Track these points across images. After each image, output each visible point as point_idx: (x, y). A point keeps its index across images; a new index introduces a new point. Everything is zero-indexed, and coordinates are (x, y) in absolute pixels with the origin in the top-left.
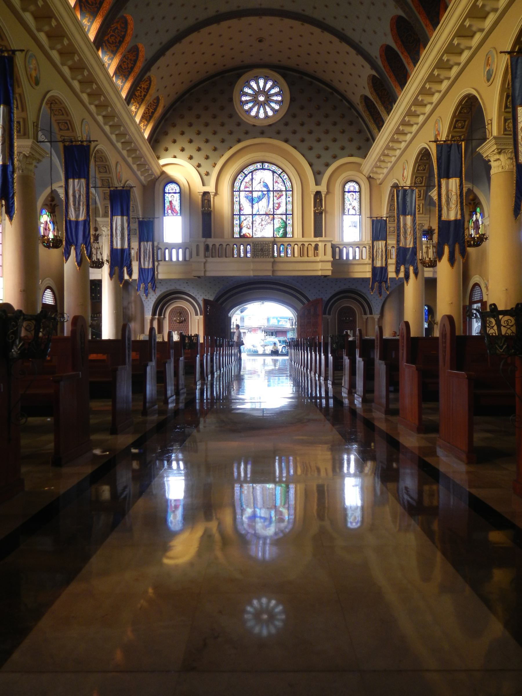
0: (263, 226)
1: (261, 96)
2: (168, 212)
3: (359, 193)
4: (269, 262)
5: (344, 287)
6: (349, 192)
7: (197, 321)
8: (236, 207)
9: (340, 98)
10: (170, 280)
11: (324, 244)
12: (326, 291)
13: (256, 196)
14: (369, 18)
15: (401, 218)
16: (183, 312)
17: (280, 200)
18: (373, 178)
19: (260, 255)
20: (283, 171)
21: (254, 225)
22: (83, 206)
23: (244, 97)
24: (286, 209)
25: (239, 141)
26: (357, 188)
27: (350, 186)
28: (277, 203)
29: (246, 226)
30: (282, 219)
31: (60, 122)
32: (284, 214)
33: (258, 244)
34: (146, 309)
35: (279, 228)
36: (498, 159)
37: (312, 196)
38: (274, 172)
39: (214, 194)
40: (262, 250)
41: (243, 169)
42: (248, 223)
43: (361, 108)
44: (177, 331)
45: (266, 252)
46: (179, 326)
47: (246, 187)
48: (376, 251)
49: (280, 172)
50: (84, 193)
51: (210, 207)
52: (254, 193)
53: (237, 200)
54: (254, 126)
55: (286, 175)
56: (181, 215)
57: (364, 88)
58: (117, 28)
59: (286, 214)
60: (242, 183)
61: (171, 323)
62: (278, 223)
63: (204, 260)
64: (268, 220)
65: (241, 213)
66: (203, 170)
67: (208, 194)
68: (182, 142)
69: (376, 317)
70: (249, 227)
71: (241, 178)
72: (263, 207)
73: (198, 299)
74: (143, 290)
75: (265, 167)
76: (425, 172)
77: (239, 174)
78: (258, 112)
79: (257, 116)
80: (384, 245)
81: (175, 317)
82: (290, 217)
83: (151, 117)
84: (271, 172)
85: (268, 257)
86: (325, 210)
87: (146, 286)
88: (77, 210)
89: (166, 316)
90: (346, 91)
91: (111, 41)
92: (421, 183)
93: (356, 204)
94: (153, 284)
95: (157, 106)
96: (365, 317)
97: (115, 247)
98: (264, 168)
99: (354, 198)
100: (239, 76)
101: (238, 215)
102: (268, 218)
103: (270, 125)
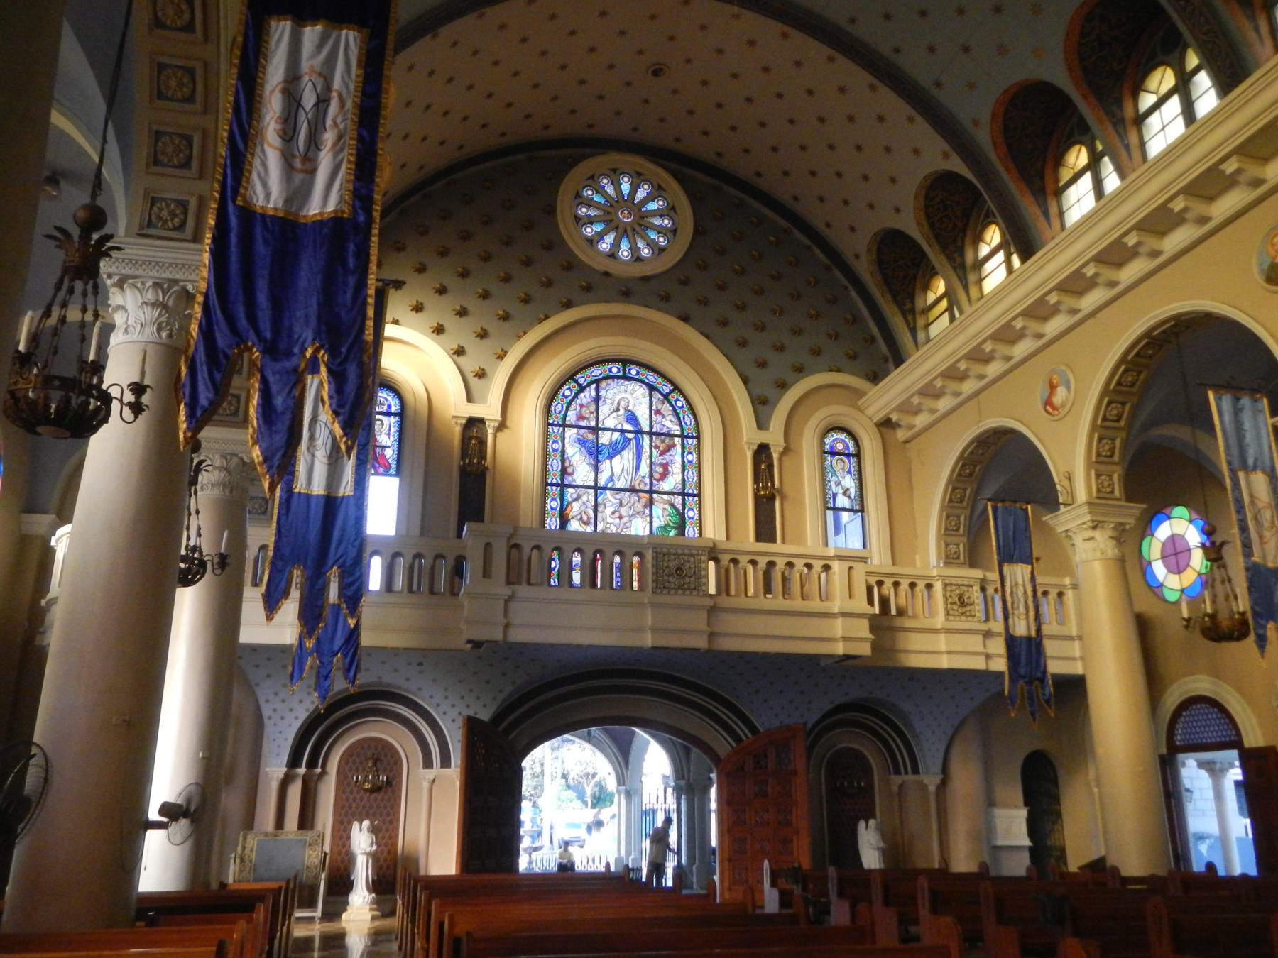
0: (625, 520)
1: (626, 212)
4: (699, 608)
5: (856, 693)
6: (833, 453)
7: (426, 785)
8: (555, 464)
10: (384, 648)
11: (846, 565)
12: (809, 702)
13: (607, 443)
15: (1241, 475)
17: (667, 457)
20: (676, 388)
21: (599, 515)
22: (338, 148)
23: (584, 210)
24: (683, 480)
25: (568, 305)
27: (834, 441)
28: (661, 464)
29: (579, 517)
30: (673, 505)
32: (678, 494)
33: (669, 554)
34: (268, 747)
37: (749, 454)
38: (651, 388)
39: (496, 424)
42: (583, 508)
43: (865, 268)
44: (367, 817)
45: (690, 577)
46: (369, 801)
47: (581, 417)
48: (1012, 593)
49: (666, 390)
50: (352, 86)
51: (483, 455)
52: (600, 432)
54: (607, 274)
56: (398, 473)
57: (897, 210)
59: (683, 494)
61: (344, 792)
62: (661, 515)
63: (507, 591)
64: (636, 505)
65: (566, 482)
66: (470, 363)
67: (480, 425)
69: (932, 781)
70: (585, 518)
71: (567, 393)
72: (625, 472)
74: (312, 681)
75: (630, 372)
76: (1134, 390)
78: (616, 245)
79: (612, 255)
80: (1029, 576)
81: (357, 770)
82: (689, 500)
84: (644, 386)
85: (698, 595)
86: (780, 491)
87: (326, 661)
88: (298, 163)
90: (828, 225)
92: (1118, 421)
93: (849, 482)
94: (348, 659)
96: (896, 780)
97: (300, 486)
101: (557, 485)
102: (636, 498)
103: (646, 279)
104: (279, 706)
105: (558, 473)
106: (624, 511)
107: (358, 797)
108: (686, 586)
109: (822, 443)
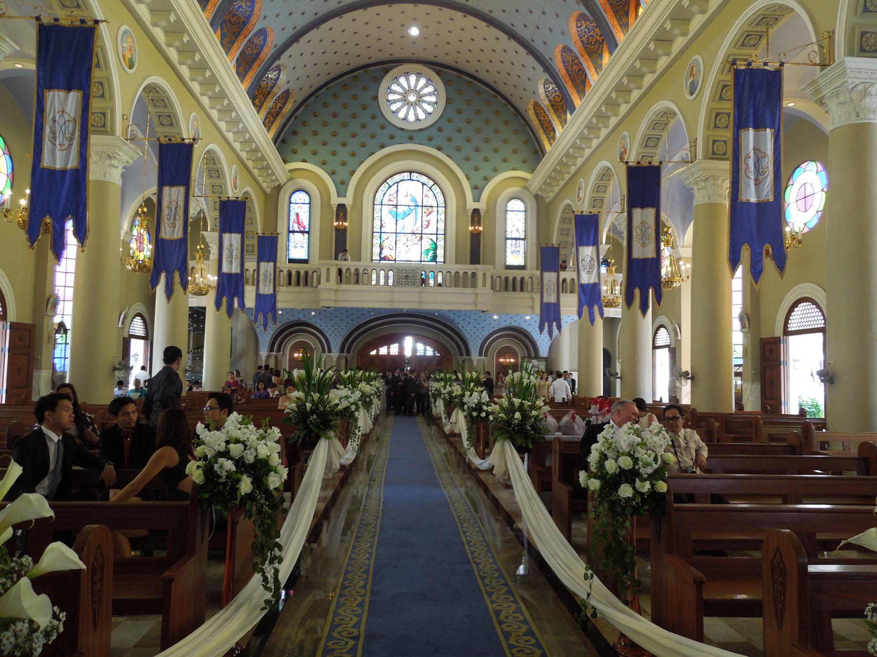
6: (512, 211)
8: (377, 224)
9: (505, 102)
14: (544, 13)
17: (429, 217)
18: (541, 197)
24: (437, 228)
30: (431, 240)
31: (161, 116)
33: (402, 270)
34: (261, 344)
35: (428, 250)
36: (705, 188)
38: (423, 184)
40: (407, 277)
41: (387, 180)
42: (390, 243)
52: (398, 207)
55: (437, 188)
58: (241, 6)
59: (437, 234)
60: (385, 195)
62: (427, 244)
68: (314, 143)
70: (391, 248)
71: (384, 189)
73: (325, 333)
77: (382, 184)
79: (405, 119)
83: (278, 113)
91: (233, 23)
95: (286, 101)
98: (412, 178)
100: (387, 71)
103: (421, 130)
105: (379, 227)
106: (409, 243)
109: (506, 206)
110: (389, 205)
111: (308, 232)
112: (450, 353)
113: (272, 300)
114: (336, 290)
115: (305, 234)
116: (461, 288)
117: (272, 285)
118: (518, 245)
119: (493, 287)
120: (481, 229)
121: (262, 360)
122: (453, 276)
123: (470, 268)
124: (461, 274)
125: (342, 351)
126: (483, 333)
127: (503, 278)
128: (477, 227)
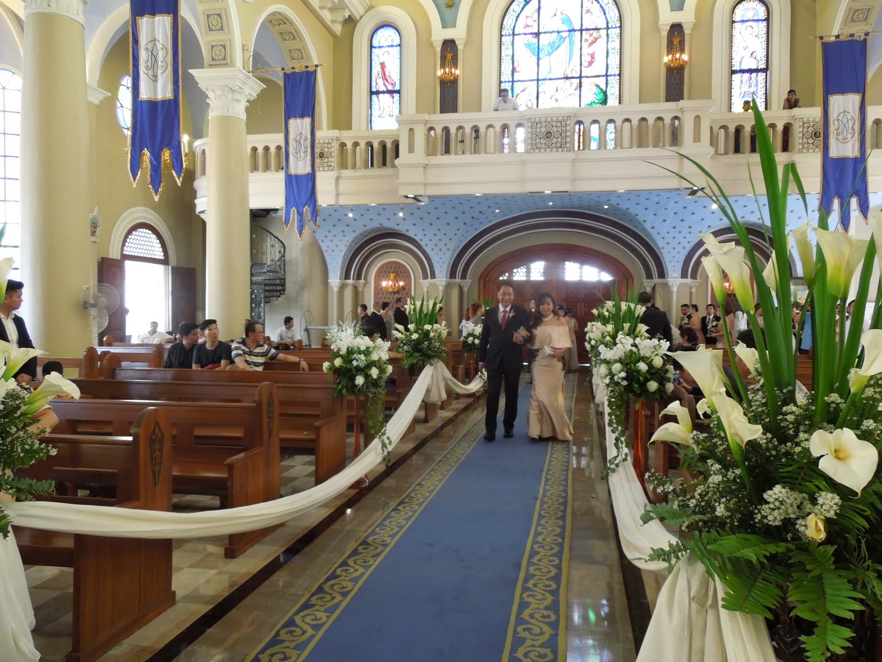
2: (377, 84)
3: (765, 23)
6: (743, 21)
8: (507, 67)
12: (690, 227)
13: (547, 44)
16: (401, 272)
19: (544, 145)
24: (607, 65)
26: (761, 12)
27: (745, 10)
28: (589, 54)
30: (597, 86)
33: (540, 122)
52: (541, 36)
53: (507, 54)
59: (607, 76)
61: (379, 294)
62: (590, 94)
85: (563, 151)
89: (368, 280)
99: (755, 32)
104: (330, 244)
107: (387, 296)
108: (553, 145)
110: (525, 34)
111: (398, 92)
112: (631, 275)
113: (310, 185)
114: (426, 167)
115: (395, 95)
116: (651, 148)
117: (309, 157)
118: (753, 81)
119: (713, 141)
120: (685, 57)
121: (333, 292)
122: (634, 128)
123: (668, 109)
124: (651, 121)
125: (452, 274)
126: (688, 236)
127: (732, 129)
128: (678, 56)
